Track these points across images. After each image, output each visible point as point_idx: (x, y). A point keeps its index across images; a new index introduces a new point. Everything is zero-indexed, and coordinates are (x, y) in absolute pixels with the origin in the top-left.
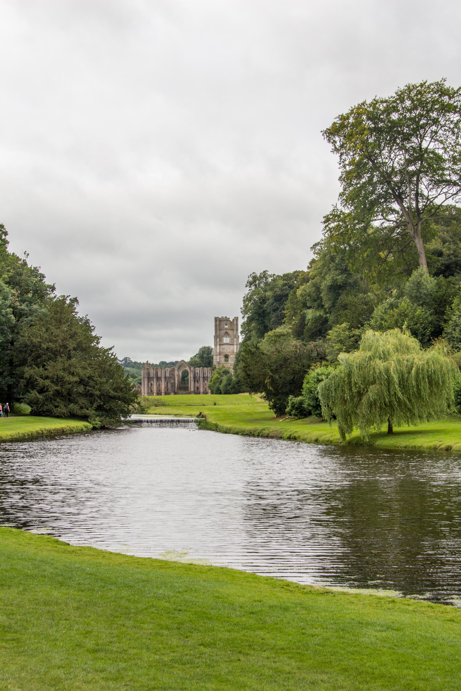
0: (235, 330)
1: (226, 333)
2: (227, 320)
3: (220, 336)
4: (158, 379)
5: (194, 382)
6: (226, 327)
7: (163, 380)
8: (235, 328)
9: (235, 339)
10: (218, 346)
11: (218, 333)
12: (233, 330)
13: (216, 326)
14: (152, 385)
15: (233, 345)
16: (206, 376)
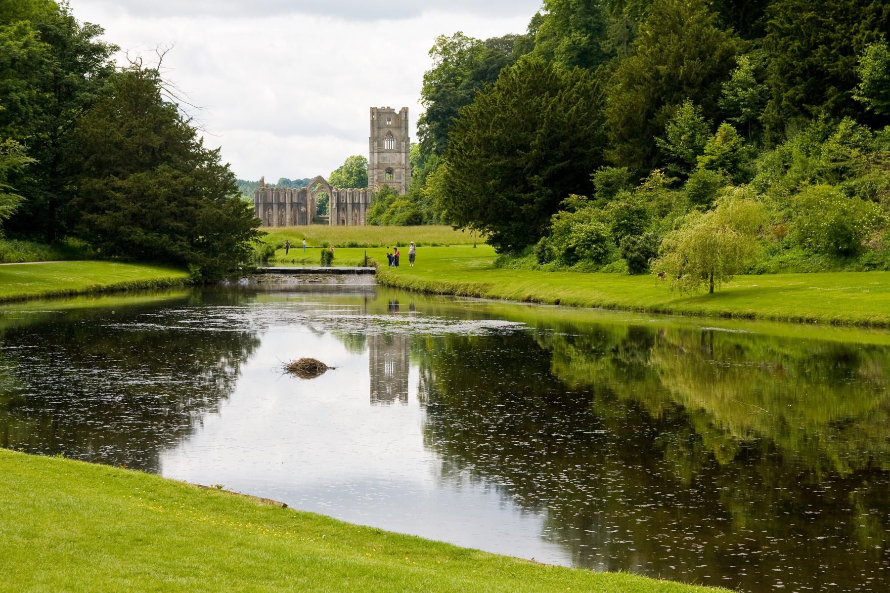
0: (403, 129)
1: (390, 133)
2: (390, 112)
3: (378, 136)
4: (282, 206)
5: (338, 211)
6: (390, 123)
7: (288, 207)
8: (403, 125)
9: (403, 144)
10: (376, 155)
11: (376, 133)
12: (399, 128)
13: (372, 122)
14: (269, 216)
15: (400, 152)
16: (357, 201)
